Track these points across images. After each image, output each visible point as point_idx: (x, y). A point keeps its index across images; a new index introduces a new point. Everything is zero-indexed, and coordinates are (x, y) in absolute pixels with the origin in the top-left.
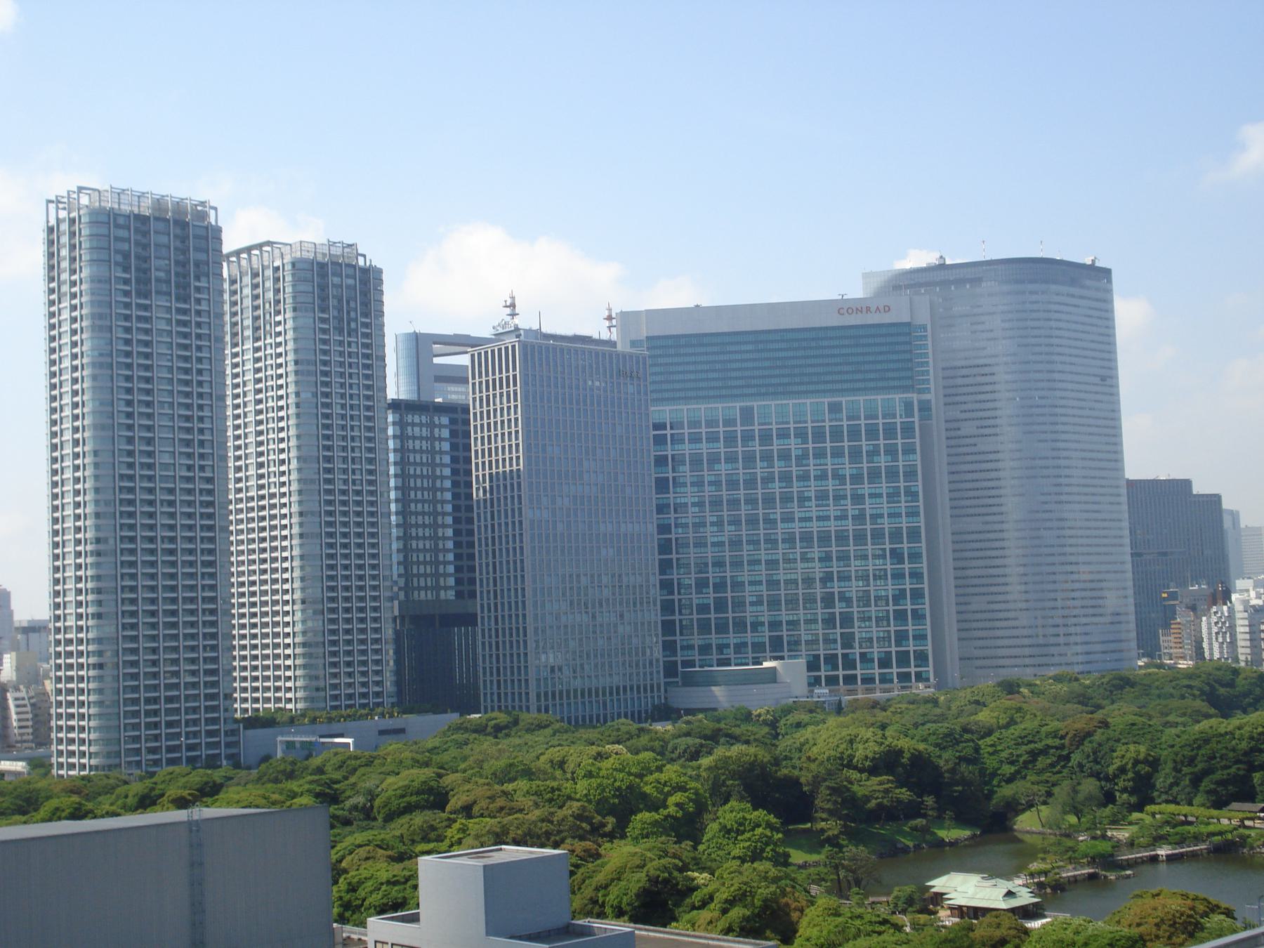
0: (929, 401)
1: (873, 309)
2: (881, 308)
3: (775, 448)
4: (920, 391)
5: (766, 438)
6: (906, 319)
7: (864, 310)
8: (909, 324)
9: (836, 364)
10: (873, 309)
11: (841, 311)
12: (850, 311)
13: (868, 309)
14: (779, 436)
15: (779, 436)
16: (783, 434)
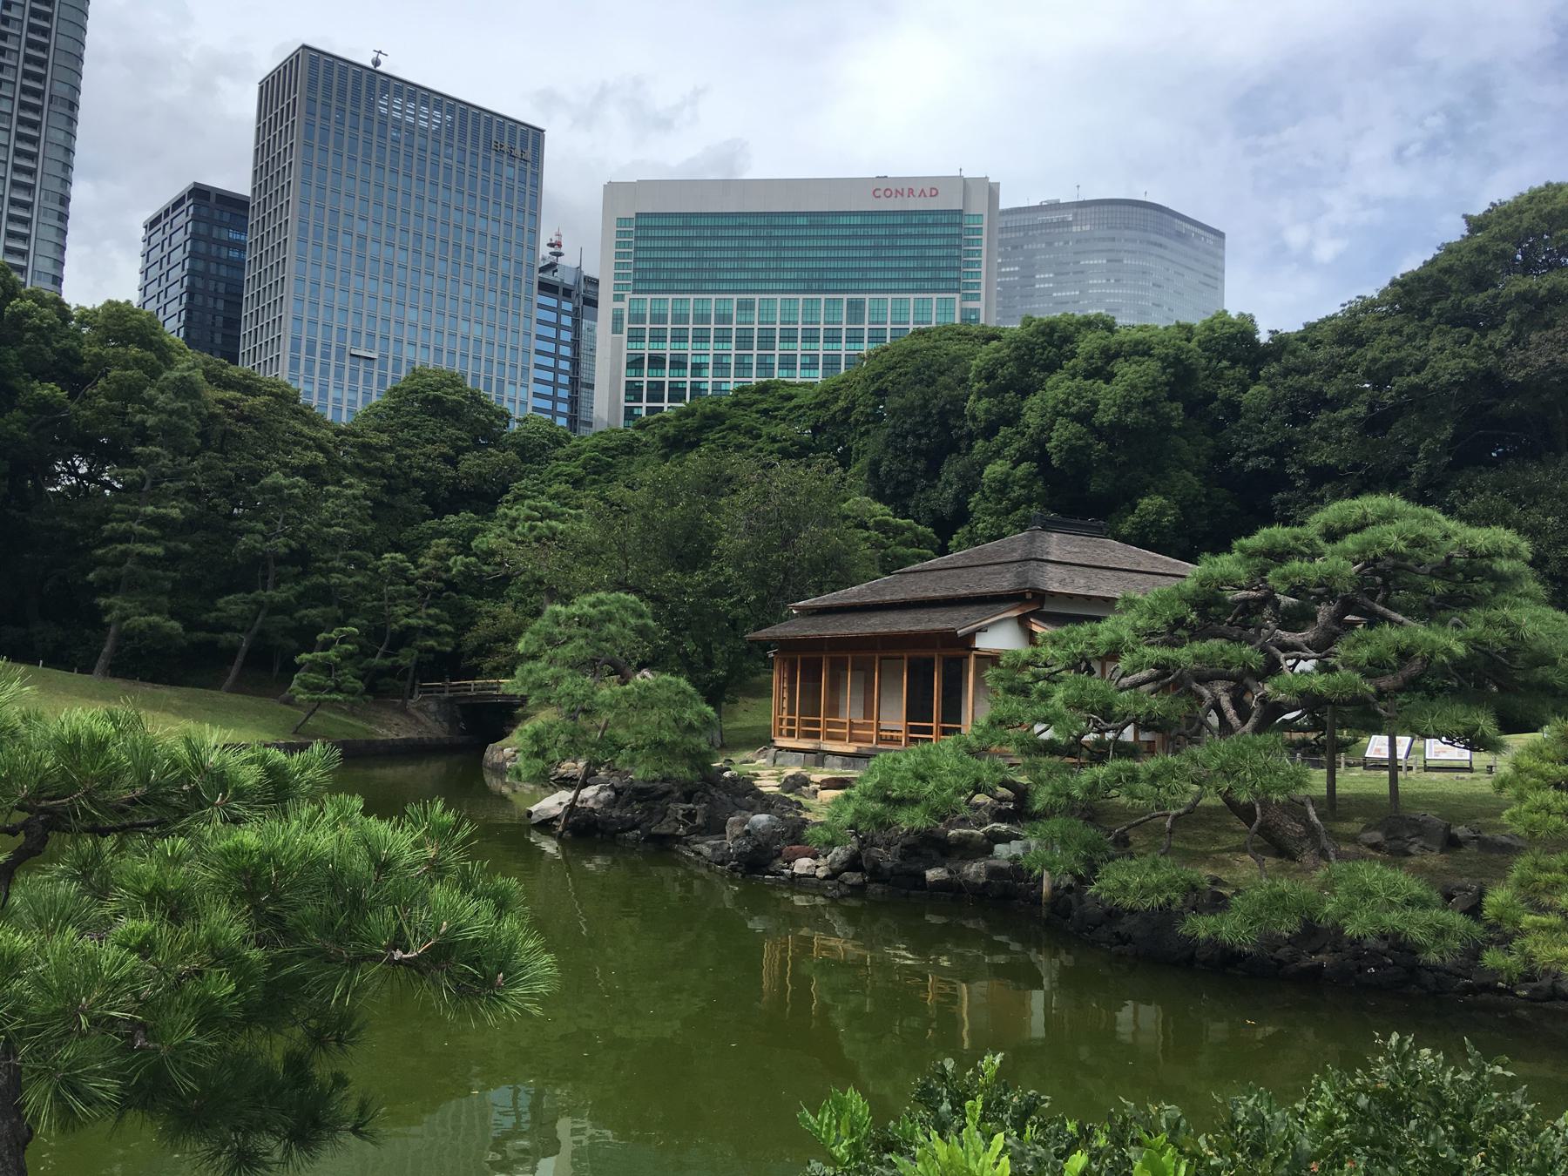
0: (976, 311)
1: (917, 193)
2: (927, 192)
3: (777, 352)
4: (966, 298)
5: (767, 340)
6: (958, 206)
7: (906, 192)
8: (960, 212)
9: (866, 259)
10: (917, 193)
11: (877, 193)
12: (888, 193)
13: (911, 191)
14: (783, 339)
15: (783, 339)
16: (789, 337)
